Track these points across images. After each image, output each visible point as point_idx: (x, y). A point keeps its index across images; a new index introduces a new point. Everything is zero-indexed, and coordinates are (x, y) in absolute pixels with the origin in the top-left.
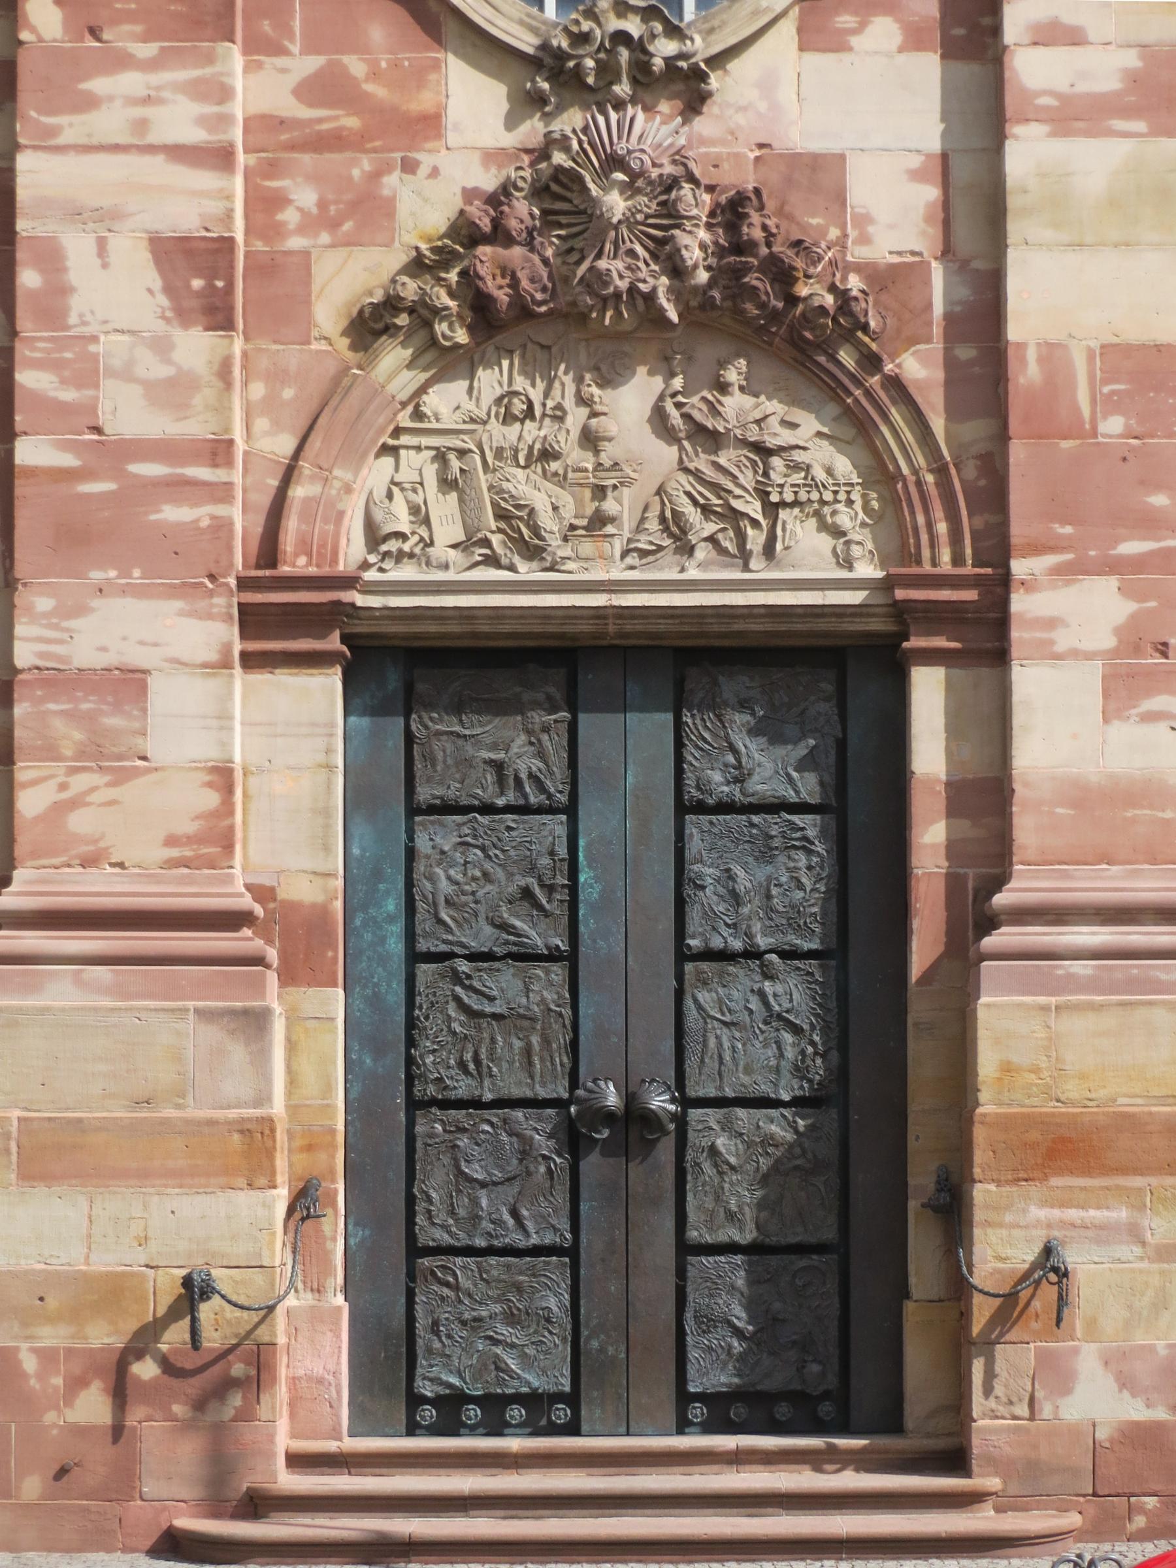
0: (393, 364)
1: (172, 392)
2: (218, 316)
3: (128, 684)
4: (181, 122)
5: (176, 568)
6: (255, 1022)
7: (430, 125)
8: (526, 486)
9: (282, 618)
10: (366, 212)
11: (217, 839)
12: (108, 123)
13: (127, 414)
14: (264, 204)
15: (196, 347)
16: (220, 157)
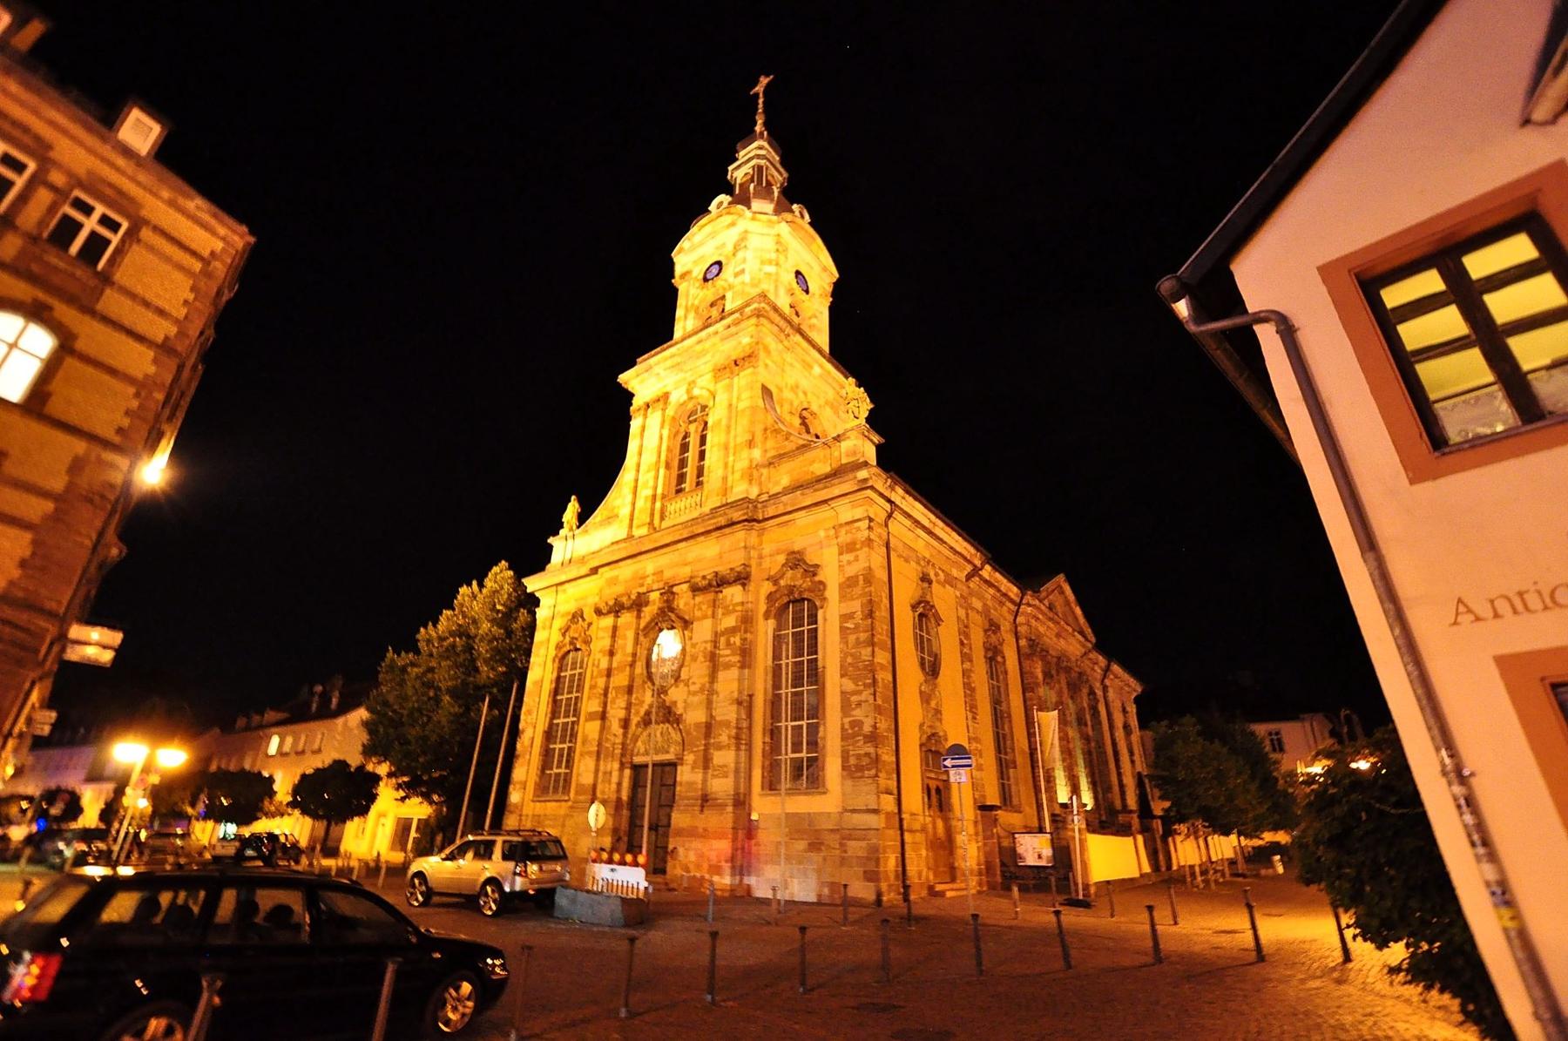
10: (637, 712)
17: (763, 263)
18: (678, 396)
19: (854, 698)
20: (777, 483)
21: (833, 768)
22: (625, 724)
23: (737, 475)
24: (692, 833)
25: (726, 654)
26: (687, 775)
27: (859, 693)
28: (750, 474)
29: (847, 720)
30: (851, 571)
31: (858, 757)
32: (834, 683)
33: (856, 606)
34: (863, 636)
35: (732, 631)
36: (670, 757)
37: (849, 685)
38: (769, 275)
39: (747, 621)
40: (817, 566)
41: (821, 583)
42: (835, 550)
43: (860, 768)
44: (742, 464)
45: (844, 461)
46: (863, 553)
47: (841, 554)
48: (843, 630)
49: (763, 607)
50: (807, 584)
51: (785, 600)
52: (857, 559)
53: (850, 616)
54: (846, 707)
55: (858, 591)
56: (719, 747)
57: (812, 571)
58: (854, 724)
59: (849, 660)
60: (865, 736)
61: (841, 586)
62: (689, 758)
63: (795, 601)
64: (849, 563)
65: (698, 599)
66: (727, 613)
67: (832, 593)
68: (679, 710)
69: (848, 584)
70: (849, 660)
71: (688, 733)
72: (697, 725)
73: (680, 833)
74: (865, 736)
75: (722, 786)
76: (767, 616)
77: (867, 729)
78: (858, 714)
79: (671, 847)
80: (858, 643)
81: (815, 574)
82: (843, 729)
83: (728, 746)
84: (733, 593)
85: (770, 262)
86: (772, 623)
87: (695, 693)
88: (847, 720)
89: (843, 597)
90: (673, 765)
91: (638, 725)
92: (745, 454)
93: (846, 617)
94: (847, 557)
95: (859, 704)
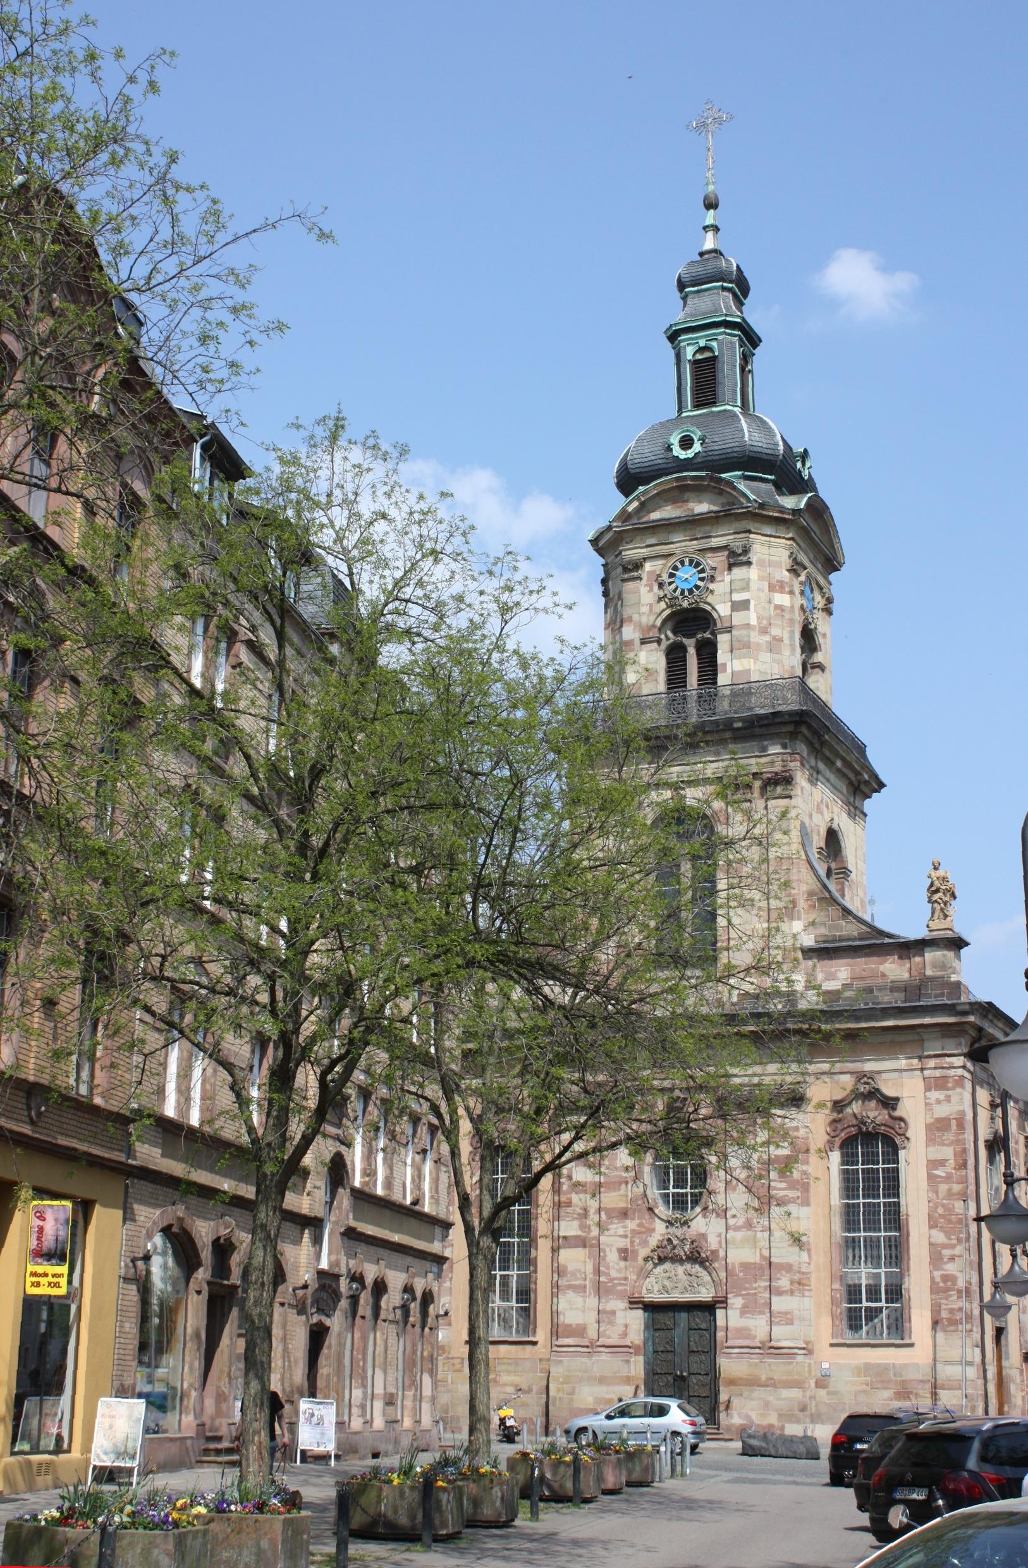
0: (650, 1265)
1: (619, 1271)
2: (625, 1259)
3: (613, 1313)
4: (621, 1232)
5: (620, 1295)
6: (628, 1362)
7: (653, 1230)
8: (666, 1283)
9: (635, 1303)
10: (645, 1243)
11: (625, 1335)
12: (611, 1232)
13: (614, 1274)
14: (632, 1242)
15: (622, 1264)
16: (625, 1236)
17: (772, 588)
19: (946, 1252)
20: (830, 977)
21: (919, 1320)
22: (625, 1254)
24: (753, 1382)
25: (780, 1188)
26: (729, 1319)
27: (953, 1247)
29: (937, 1274)
30: (942, 1111)
31: (951, 1311)
32: (920, 1235)
33: (948, 1153)
34: (957, 1188)
36: (705, 1294)
37: (939, 1237)
38: (779, 607)
40: (897, 1099)
41: (901, 1119)
42: (921, 1085)
43: (953, 1322)
45: (929, 972)
46: (955, 1094)
47: (928, 1089)
48: (931, 1178)
51: (854, 1130)
52: (948, 1099)
53: (942, 1163)
54: (936, 1259)
55: (950, 1136)
56: (780, 1293)
57: (889, 1103)
58: (946, 1278)
59: (940, 1210)
60: (959, 1292)
61: (929, 1127)
62: (736, 1302)
64: (938, 1102)
67: (917, 1131)
68: (713, 1243)
69: (938, 1128)
70: (940, 1210)
71: (733, 1274)
72: (745, 1266)
73: (732, 1382)
74: (959, 1292)
75: (783, 1335)
77: (961, 1284)
78: (951, 1268)
79: (723, 1397)
80: (950, 1195)
81: (894, 1109)
82: (932, 1279)
83: (792, 1292)
85: (781, 589)
86: (836, 1157)
87: (737, 1229)
88: (937, 1274)
89: (931, 1141)
90: (708, 1308)
91: (646, 1259)
93: (934, 1164)
94: (935, 1095)
95: (952, 1259)
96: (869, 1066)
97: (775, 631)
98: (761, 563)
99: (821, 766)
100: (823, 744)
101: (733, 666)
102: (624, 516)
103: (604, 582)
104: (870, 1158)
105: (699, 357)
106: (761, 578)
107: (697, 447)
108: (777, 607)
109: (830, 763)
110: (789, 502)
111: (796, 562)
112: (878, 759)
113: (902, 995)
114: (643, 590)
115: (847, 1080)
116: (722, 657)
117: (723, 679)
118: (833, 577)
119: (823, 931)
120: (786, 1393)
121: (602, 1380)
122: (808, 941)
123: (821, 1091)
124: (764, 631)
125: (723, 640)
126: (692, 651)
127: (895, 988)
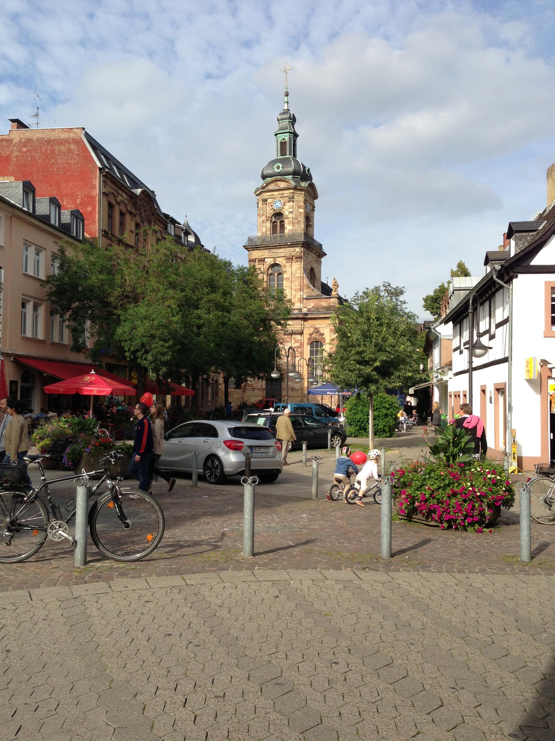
17: (298, 208)
18: (269, 261)
20: (309, 305)
23: (297, 300)
28: (301, 300)
35: (298, 347)
39: (302, 345)
42: (328, 330)
44: (298, 296)
49: (306, 341)
50: (320, 338)
63: (316, 342)
65: (285, 337)
66: (296, 342)
76: (308, 344)
84: (298, 337)
85: (301, 208)
86: (309, 346)
92: (299, 293)
96: (317, 326)
97: (299, 219)
98: (296, 201)
99: (309, 253)
100: (310, 247)
101: (288, 228)
102: (263, 188)
103: (258, 203)
104: (317, 347)
105: (282, 141)
106: (296, 205)
107: (281, 169)
108: (300, 212)
109: (312, 251)
110: (304, 184)
111: (305, 200)
112: (325, 249)
113: (325, 310)
114: (267, 207)
115: (312, 329)
116: (286, 226)
117: (286, 231)
118: (315, 201)
119: (308, 294)
120: (297, 399)
121: (256, 396)
122: (305, 296)
123: (307, 332)
124: (296, 219)
125: (286, 221)
126: (279, 223)
127: (324, 308)
